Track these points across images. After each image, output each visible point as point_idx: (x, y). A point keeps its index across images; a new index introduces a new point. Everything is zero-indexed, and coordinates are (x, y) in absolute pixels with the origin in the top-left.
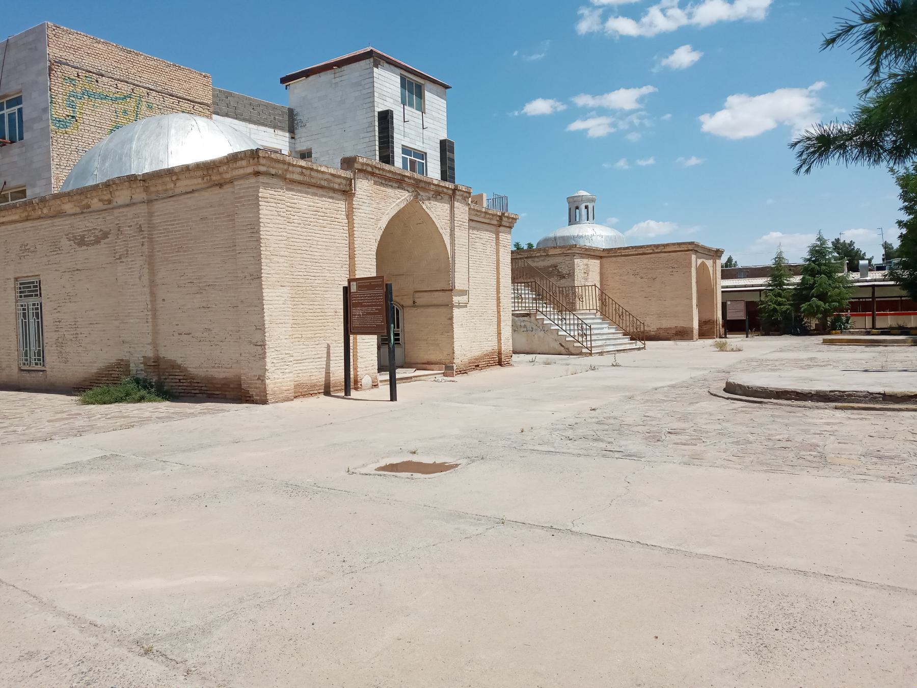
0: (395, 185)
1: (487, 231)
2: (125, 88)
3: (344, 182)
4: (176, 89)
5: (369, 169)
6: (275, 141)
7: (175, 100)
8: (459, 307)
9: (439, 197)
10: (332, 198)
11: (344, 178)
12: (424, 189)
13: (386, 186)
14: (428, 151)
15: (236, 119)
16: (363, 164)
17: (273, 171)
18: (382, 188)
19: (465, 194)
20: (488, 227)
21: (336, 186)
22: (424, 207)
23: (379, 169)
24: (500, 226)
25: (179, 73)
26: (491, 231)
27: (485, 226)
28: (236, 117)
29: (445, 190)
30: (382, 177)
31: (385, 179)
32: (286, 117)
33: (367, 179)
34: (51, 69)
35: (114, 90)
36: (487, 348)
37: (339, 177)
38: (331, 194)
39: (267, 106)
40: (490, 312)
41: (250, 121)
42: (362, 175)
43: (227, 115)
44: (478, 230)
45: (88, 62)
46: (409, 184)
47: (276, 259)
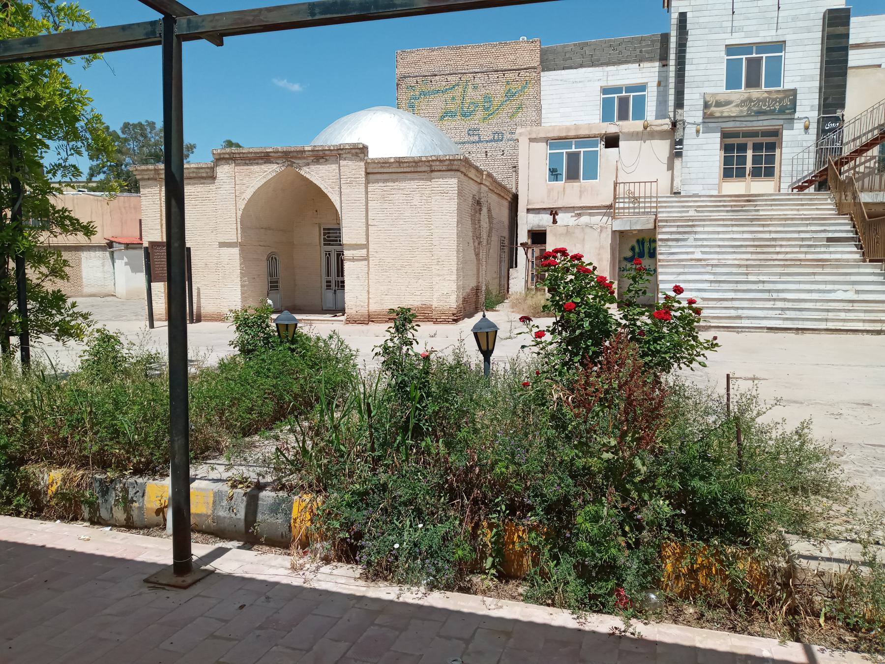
0: (260, 161)
1: (413, 179)
2: (453, 79)
3: (208, 170)
4: (502, 64)
5: (227, 156)
6: (640, 75)
7: (500, 74)
8: (353, 260)
9: (321, 161)
10: (204, 183)
11: (208, 168)
12: (300, 158)
13: (251, 164)
14: (787, 38)
15: (592, 66)
16: (220, 154)
17: (146, 177)
18: (246, 167)
19: (354, 151)
20: (416, 175)
21: (204, 175)
22: (302, 172)
23: (239, 154)
24: (432, 171)
25: (506, 49)
26: (423, 179)
27: (409, 175)
28: (593, 65)
29: (327, 152)
30: (242, 159)
31: (250, 160)
32: (658, 45)
33: (228, 164)
34: (398, 85)
35: (444, 84)
36: (411, 302)
37: (202, 168)
38: (202, 181)
39: (631, 41)
40: (417, 265)
41: (608, 64)
42: (223, 162)
43: (581, 66)
44: (394, 181)
45: (425, 69)
46: (279, 158)
47: (152, 231)
